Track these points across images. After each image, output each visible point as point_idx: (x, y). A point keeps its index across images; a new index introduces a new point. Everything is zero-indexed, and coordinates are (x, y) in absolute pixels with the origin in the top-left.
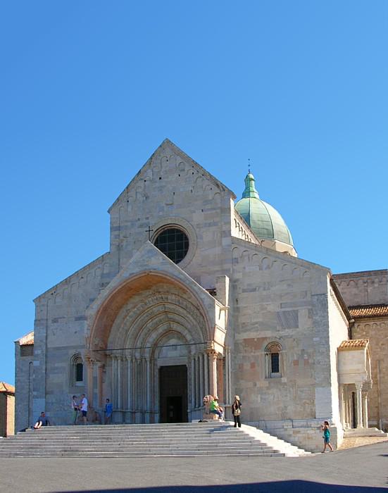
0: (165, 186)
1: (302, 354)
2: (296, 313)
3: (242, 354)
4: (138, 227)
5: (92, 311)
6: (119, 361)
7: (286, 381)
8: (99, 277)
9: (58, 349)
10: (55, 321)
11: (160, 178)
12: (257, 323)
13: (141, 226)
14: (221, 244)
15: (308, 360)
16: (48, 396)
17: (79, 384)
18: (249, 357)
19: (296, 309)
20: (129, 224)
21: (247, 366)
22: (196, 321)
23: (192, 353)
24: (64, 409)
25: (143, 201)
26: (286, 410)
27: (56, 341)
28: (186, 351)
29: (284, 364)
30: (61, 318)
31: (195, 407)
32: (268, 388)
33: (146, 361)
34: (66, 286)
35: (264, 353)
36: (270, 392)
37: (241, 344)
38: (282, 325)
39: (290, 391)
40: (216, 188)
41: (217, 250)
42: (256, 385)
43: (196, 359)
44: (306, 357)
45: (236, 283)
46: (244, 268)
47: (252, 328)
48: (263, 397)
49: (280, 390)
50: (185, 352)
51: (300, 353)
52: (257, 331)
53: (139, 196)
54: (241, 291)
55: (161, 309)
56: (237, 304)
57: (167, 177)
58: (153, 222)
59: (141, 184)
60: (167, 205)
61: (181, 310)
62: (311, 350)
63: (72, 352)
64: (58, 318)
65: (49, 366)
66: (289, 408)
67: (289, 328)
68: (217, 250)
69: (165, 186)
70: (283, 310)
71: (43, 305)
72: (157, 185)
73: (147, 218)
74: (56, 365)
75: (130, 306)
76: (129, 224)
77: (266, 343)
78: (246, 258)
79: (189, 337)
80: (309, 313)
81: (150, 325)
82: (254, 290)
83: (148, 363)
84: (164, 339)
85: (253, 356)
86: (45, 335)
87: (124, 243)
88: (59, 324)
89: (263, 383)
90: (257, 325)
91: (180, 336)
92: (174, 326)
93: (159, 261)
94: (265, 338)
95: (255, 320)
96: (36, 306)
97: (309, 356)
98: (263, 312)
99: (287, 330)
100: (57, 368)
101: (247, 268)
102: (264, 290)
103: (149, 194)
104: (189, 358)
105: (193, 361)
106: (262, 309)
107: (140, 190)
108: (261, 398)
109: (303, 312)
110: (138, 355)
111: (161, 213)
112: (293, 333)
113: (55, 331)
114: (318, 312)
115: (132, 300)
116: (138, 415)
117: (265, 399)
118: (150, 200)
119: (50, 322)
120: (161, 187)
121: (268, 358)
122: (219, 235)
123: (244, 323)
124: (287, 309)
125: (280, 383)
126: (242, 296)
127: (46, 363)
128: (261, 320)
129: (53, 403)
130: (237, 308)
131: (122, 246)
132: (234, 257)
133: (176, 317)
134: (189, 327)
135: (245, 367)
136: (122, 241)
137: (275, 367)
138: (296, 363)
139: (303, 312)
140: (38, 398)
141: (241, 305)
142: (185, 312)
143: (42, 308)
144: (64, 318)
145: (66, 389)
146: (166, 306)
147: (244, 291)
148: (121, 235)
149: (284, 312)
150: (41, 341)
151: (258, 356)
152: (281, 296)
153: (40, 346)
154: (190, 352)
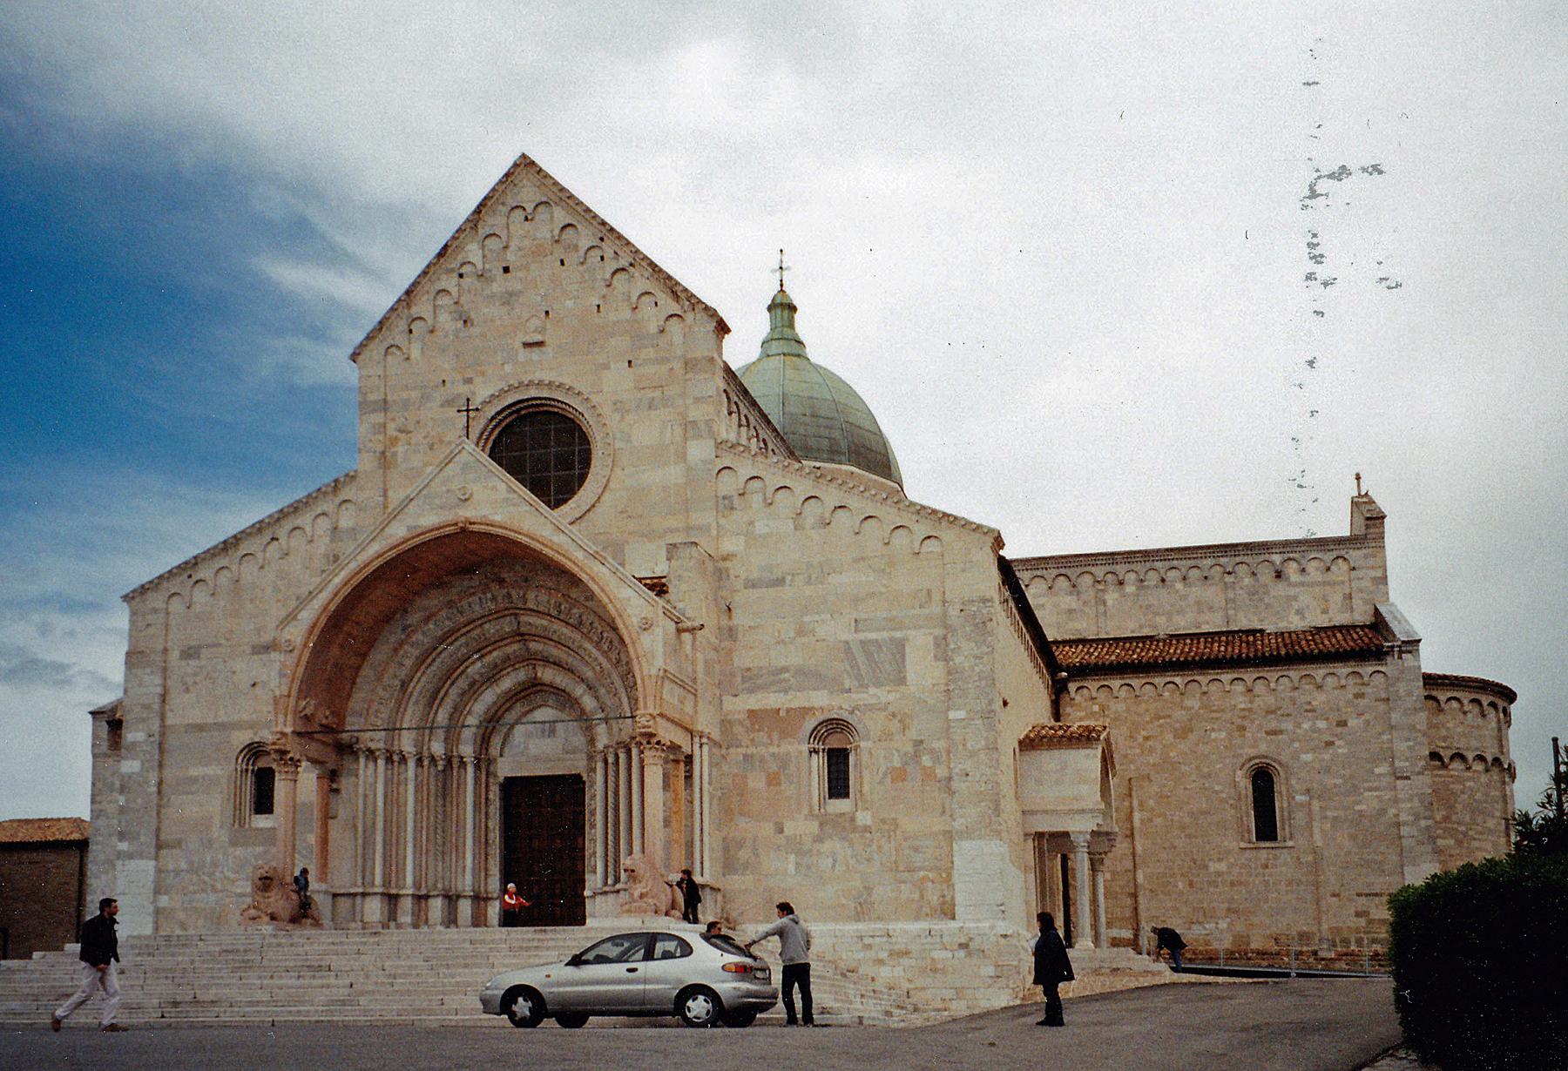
1: (916, 756)
2: (900, 647)
5: (296, 633)
7: (869, 823)
8: (327, 540)
9: (200, 728)
10: (189, 653)
11: (506, 270)
12: (785, 669)
13: (448, 403)
14: (682, 456)
15: (933, 768)
16: (164, 852)
18: (762, 760)
19: (898, 635)
20: (414, 395)
21: (757, 782)
22: (609, 659)
23: (600, 746)
24: (214, 889)
25: (457, 330)
26: (870, 895)
27: (186, 710)
29: (862, 773)
30: (208, 646)
32: (819, 839)
33: (463, 764)
34: (224, 562)
35: (805, 748)
36: (827, 846)
37: (740, 722)
38: (859, 677)
39: (880, 847)
40: (670, 301)
42: (781, 831)
43: (611, 760)
44: (926, 760)
45: (728, 564)
46: (751, 523)
47: (772, 683)
49: (852, 845)
50: (579, 740)
51: (910, 749)
52: (786, 691)
53: (444, 317)
54: (739, 585)
55: (507, 625)
57: (526, 268)
59: (449, 282)
61: (566, 631)
62: (940, 745)
64: (200, 647)
65: (168, 773)
66: (878, 891)
67: (878, 684)
68: (674, 474)
70: (861, 636)
71: (155, 611)
73: (469, 381)
74: (194, 772)
75: (414, 618)
76: (414, 395)
77: (810, 724)
78: (757, 499)
79: (588, 702)
80: (937, 645)
81: (475, 669)
82: (780, 582)
84: (518, 709)
85: (773, 755)
86: (159, 690)
87: (400, 449)
89: (801, 827)
90: (787, 675)
91: (565, 700)
92: (547, 674)
93: (500, 503)
94: (805, 711)
95: (783, 663)
96: (133, 614)
97: (937, 759)
98: (805, 640)
99: (872, 690)
100: (194, 780)
102: (809, 582)
103: (473, 315)
104: (591, 758)
105: (600, 766)
106: (801, 632)
109: (920, 643)
110: (438, 748)
111: (508, 368)
112: (891, 697)
113: (190, 680)
114: (964, 644)
115: (421, 602)
116: (437, 906)
117: (809, 867)
119: (174, 655)
120: (511, 294)
121: (819, 764)
123: (749, 669)
124: (872, 636)
125: (853, 819)
126: (741, 598)
127: (161, 766)
129: (177, 873)
130: (731, 629)
131: (395, 454)
132: (720, 494)
133: (555, 652)
134: (589, 674)
135: (751, 784)
136: (394, 441)
137: (838, 786)
138: (899, 775)
139: (920, 643)
141: (740, 619)
142: (577, 636)
146: (524, 619)
147: (751, 584)
148: (391, 426)
149: (863, 643)
150: (146, 707)
151: (788, 754)
152: (856, 600)
154: (592, 741)
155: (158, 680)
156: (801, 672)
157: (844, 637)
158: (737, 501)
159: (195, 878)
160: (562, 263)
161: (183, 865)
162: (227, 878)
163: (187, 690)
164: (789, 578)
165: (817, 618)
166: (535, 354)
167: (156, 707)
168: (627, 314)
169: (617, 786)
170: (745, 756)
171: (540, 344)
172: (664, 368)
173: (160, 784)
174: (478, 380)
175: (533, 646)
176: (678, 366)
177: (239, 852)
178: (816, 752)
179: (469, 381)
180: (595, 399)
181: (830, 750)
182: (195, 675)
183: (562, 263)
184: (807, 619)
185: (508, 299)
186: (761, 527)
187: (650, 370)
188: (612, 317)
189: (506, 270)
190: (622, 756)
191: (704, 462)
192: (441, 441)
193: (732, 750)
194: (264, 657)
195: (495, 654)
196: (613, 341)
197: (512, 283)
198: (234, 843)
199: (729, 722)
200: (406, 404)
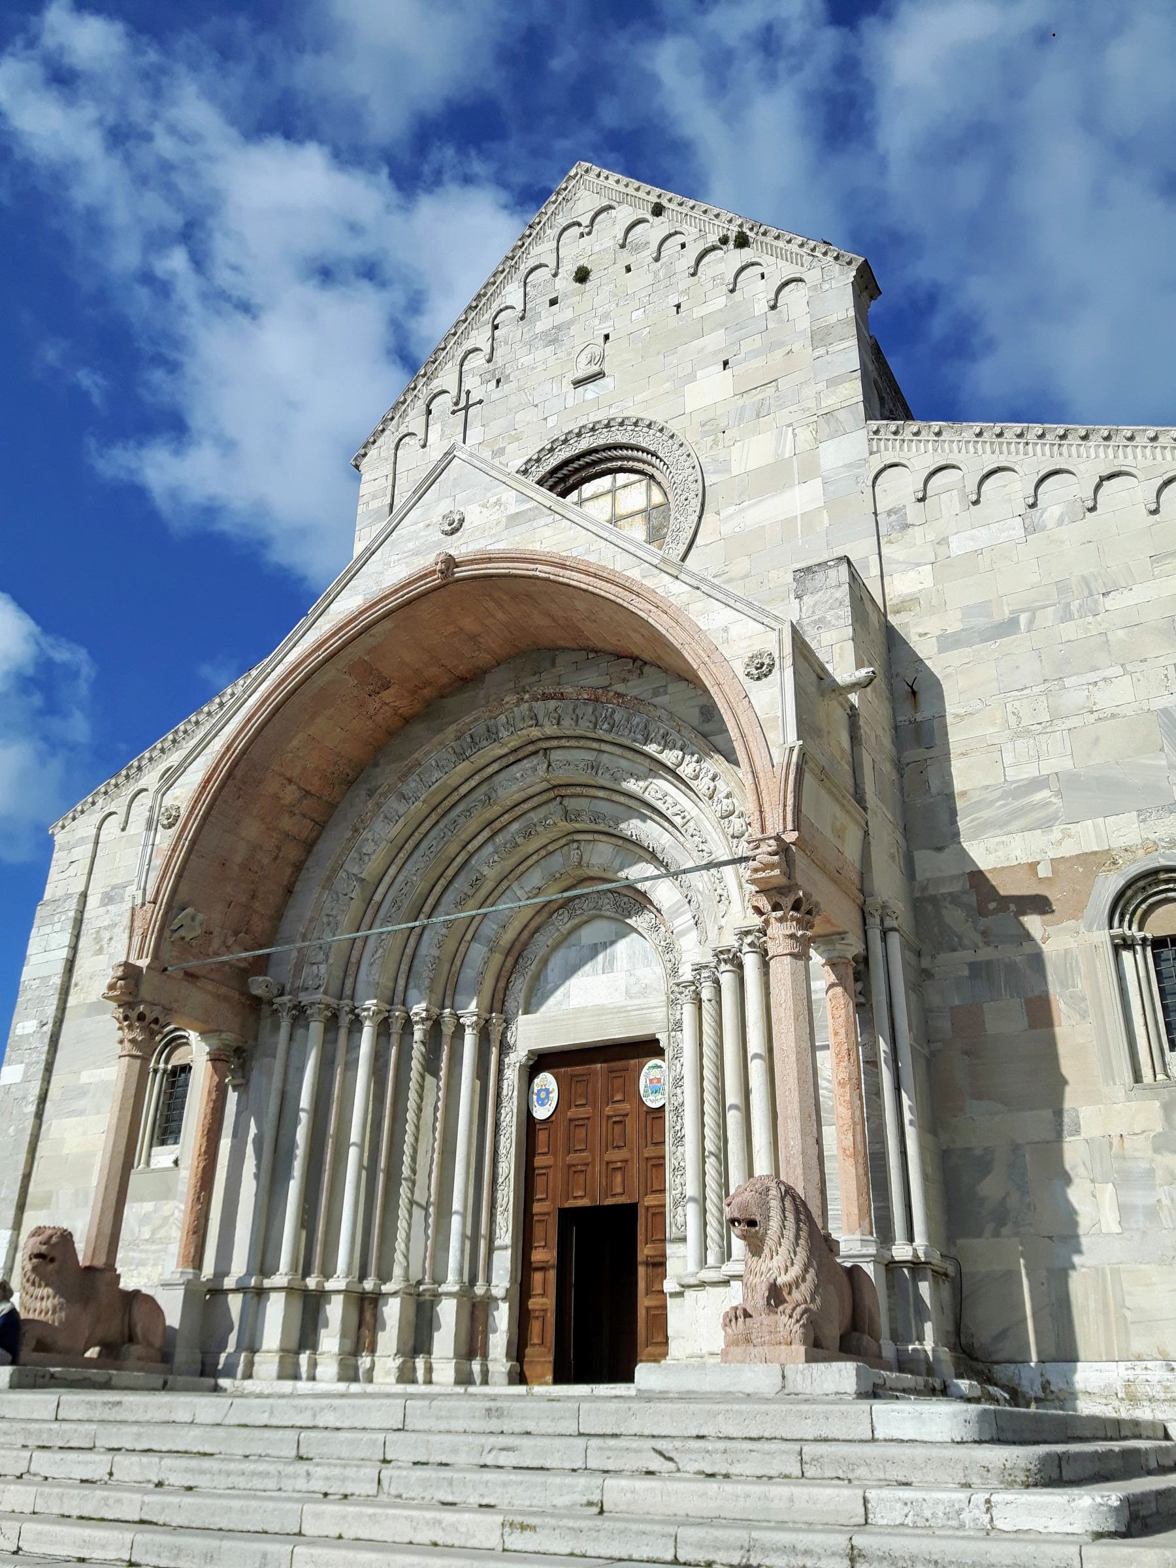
0: (571, 322)
3: (967, 955)
6: (316, 1028)
12: (1037, 784)
18: (1011, 968)
28: (659, 970)
31: (703, 1262)
35: (1102, 937)
37: (954, 899)
41: (803, 498)
43: (706, 994)
46: (943, 541)
47: (1015, 815)
48: (1139, 1198)
52: (1046, 825)
56: (916, 707)
60: (578, 383)
69: (571, 322)
72: (540, 327)
74: (86, 1077)
77: (1112, 883)
82: (1009, 627)
83: (470, 1041)
84: (563, 923)
86: (64, 953)
90: (1042, 795)
94: (1095, 861)
95: (1029, 772)
101: (954, 542)
102: (1066, 616)
107: (477, 362)
108: (1124, 1210)
111: (551, 422)
117: (1152, 1213)
118: (505, 388)
119: (93, 901)
120: (558, 328)
122: (805, 435)
128: (1067, 764)
155: (66, 938)
156: (1067, 783)
157: (1158, 704)
158: (913, 512)
160: (628, 269)
164: (1023, 618)
165: (1092, 677)
166: (591, 390)
167: (57, 981)
168: (719, 301)
169: (720, 1036)
170: (973, 966)
172: (779, 353)
173: (43, 1099)
174: (510, 449)
175: (572, 804)
176: (801, 346)
178: (1122, 945)
179: (502, 451)
180: (673, 427)
181: (1158, 943)
183: (628, 269)
184: (1068, 682)
185: (553, 338)
186: (958, 546)
187: (758, 363)
188: (698, 312)
190: (727, 980)
191: (849, 466)
193: (943, 957)
195: (515, 826)
196: (697, 344)
197: (561, 314)
199: (933, 900)
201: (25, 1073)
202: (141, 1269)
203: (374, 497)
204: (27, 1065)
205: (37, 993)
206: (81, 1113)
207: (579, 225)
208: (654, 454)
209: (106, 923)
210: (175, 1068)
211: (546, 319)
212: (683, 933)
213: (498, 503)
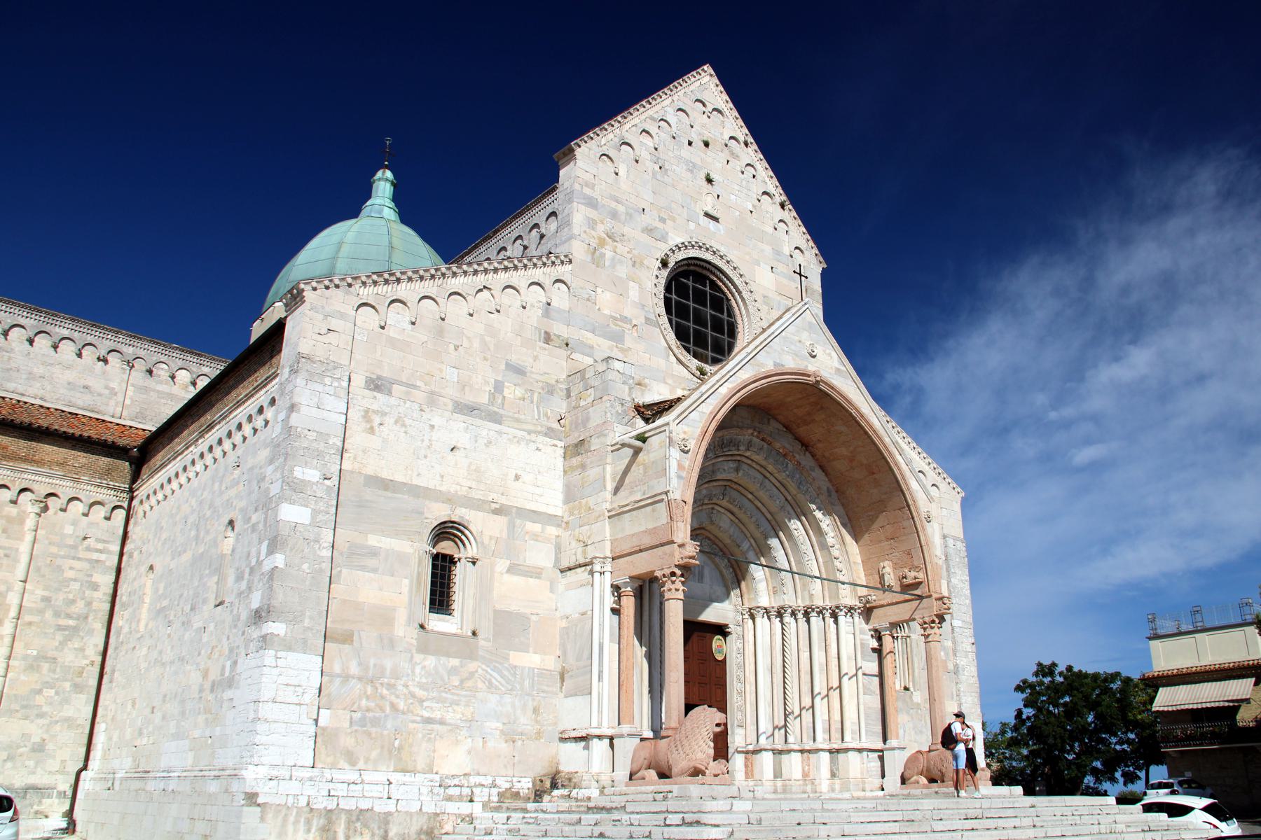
4: (643, 231)
9: (386, 485)
10: (377, 385)
11: (690, 143)
13: (649, 231)
17: (438, 623)
24: (393, 705)
30: (401, 383)
58: (679, 240)
60: (707, 215)
63: (439, 513)
71: (342, 316)
73: (663, 220)
74: (373, 541)
88: (393, 401)
100: (374, 552)
111: (692, 226)
113: (377, 420)
129: (346, 678)
136: (602, 243)
140: (289, 648)
143: (334, 323)
144: (415, 387)
145: (404, 631)
148: (601, 229)
153: (320, 455)
159: (369, 690)
161: (354, 669)
162: (413, 695)
163: (372, 430)
171: (716, 219)
177: (431, 661)
180: (752, 287)
182: (384, 414)
189: (690, 143)
192: (642, 263)
194: (470, 420)
198: (424, 649)
200: (614, 215)
201: (313, 518)
202: (455, 707)
203: (587, 185)
204: (313, 510)
205: (315, 445)
206: (374, 570)
207: (704, 105)
208: (740, 293)
209: (375, 407)
210: (438, 554)
211: (686, 152)
212: (760, 581)
213: (829, 355)
